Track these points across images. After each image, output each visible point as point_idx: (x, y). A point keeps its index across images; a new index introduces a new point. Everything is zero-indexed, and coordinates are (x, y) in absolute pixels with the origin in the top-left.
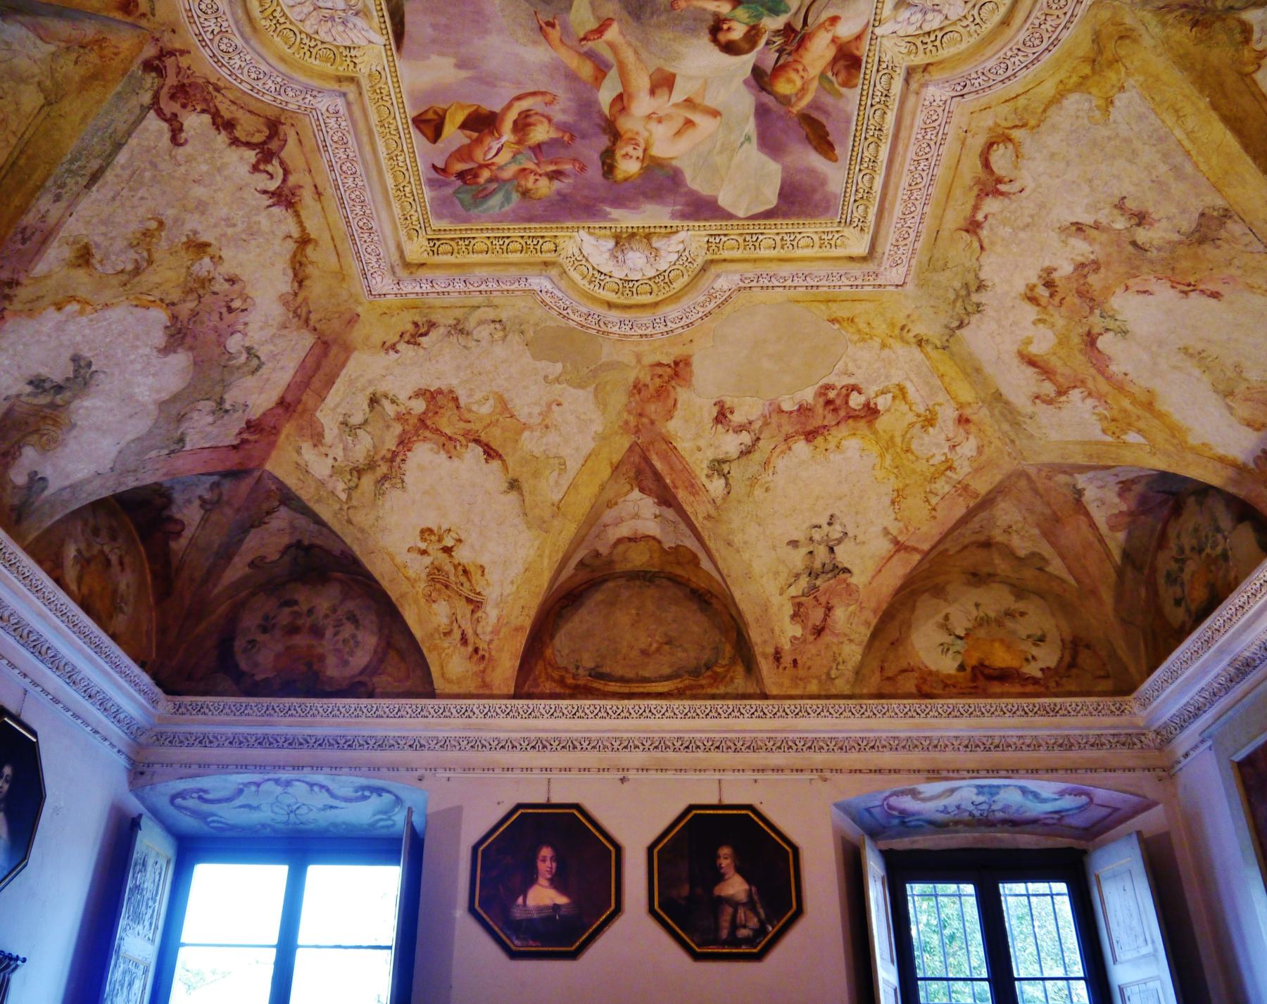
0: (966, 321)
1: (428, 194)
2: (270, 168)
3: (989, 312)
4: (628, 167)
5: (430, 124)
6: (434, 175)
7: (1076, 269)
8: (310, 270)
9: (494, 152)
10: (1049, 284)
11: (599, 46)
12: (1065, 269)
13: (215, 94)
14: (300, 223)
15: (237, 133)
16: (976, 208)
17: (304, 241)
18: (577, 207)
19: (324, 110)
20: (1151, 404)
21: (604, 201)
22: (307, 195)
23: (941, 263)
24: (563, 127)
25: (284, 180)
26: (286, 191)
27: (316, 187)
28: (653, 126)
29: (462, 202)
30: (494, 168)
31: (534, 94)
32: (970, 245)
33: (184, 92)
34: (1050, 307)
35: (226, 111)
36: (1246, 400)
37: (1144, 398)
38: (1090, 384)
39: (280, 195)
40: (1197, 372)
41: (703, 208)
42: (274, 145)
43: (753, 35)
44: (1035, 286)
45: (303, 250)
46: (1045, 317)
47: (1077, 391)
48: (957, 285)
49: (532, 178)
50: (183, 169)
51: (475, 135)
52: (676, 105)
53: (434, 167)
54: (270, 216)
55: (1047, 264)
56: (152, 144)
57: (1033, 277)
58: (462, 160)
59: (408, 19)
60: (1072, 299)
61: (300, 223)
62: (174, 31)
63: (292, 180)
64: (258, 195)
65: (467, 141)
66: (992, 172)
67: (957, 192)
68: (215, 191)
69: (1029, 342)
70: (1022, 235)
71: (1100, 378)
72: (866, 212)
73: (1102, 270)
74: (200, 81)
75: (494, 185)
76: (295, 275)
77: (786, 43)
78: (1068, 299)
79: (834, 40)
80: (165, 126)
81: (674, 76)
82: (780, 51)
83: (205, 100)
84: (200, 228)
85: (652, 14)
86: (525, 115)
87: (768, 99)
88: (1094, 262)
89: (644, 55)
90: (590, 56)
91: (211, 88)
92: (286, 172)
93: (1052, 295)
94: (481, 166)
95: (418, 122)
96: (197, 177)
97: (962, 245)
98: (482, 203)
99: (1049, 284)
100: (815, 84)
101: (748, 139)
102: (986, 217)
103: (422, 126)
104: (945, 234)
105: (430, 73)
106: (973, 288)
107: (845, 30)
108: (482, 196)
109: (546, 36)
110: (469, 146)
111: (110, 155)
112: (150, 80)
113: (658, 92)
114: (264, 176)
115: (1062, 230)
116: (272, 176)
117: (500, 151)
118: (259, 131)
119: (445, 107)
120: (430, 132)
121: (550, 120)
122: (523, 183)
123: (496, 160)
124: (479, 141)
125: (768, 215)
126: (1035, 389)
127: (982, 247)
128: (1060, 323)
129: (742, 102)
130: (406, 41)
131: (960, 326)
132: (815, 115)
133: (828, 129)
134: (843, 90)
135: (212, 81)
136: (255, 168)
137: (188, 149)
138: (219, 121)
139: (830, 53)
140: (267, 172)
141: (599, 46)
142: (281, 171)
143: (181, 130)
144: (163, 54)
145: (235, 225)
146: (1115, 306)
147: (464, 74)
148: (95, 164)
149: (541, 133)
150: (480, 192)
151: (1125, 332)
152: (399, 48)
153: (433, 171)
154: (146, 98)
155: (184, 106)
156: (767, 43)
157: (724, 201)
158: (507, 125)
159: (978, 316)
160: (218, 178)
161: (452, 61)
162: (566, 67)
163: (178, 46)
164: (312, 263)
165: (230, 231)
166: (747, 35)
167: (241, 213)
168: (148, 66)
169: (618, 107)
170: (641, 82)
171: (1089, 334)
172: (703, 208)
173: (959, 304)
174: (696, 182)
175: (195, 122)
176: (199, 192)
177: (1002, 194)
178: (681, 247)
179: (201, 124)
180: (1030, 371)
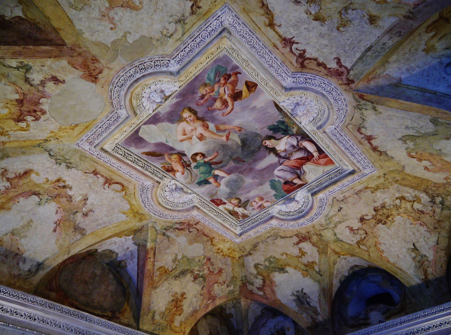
0: (52, 157)
1: (235, 62)
2: (299, 52)
3: (55, 166)
4: (186, 114)
5: (251, 86)
6: (238, 70)
7: (69, 195)
8: (262, 12)
9: (226, 90)
10: (64, 187)
11: (225, 134)
12: (70, 193)
13: (327, 74)
14: (277, 33)
15: (315, 62)
16: (102, 176)
17: (271, 25)
18: (187, 93)
19: (288, 78)
20: (3, 208)
21: (182, 101)
22: (280, 45)
23: (84, 160)
24: (214, 110)
25: (291, 48)
26: (289, 44)
27: (278, 49)
28: (192, 128)
29: (222, 67)
30: (222, 85)
31: (230, 113)
32: (88, 170)
33: (338, 74)
34: (54, 185)
35: (321, 69)
36: (12, 240)
37: (6, 206)
38: (12, 190)
39: (290, 42)
40: (21, 224)
41: (154, 120)
42: (300, 60)
43: (195, 160)
44: (65, 183)
45: (270, 21)
46: (49, 182)
47: (9, 185)
48: (72, 161)
49: (208, 91)
50: (333, 50)
51: (236, 91)
52: (193, 135)
53: (240, 73)
54: (291, 34)
55: (73, 188)
56: (347, 58)
57: (69, 182)
58: (233, 81)
59: (277, 110)
60: (56, 192)
61: (277, 33)
62: (346, 90)
63: (288, 49)
64: (299, 42)
65: (237, 88)
66: (113, 183)
67: (111, 173)
68: (318, 42)
69: (37, 174)
70: (87, 185)
71: (16, 194)
72: (120, 154)
73: (68, 202)
74: (333, 77)
75: (217, 80)
76: (267, 8)
77: (186, 164)
78: (57, 191)
79: (178, 171)
80: (343, 64)
81: (201, 141)
82: (185, 162)
83: (331, 72)
84: (320, 27)
85: (220, 148)
86: (227, 106)
87: (174, 152)
88: (71, 201)
89: (212, 140)
90: (224, 131)
91: (329, 75)
92: (291, 51)
93: (59, 187)
94: (226, 83)
95: (255, 85)
96: (327, 47)
97: (88, 167)
98: (215, 71)
99: (64, 187)
100: (169, 162)
101: (167, 142)
102: (98, 177)
103: (254, 84)
104: (96, 165)
105: (262, 100)
106: (68, 165)
107: (178, 175)
108: (217, 73)
109: (239, 127)
110: (235, 87)
111: (363, 56)
112: (351, 78)
113: (200, 135)
114: (300, 49)
115: (86, 195)
116: (296, 49)
117: (225, 91)
118: (308, 64)
119: (251, 94)
120: (250, 84)
121: (219, 110)
122: (209, 87)
123: (223, 88)
124: (233, 90)
125: (137, 132)
126: (10, 170)
127: (86, 173)
128: (46, 186)
129: (179, 147)
130: (274, 105)
131: (50, 154)
132: (161, 157)
133: (154, 158)
134: (163, 165)
135: (329, 77)
136: (304, 51)
137: (333, 57)
138: (323, 66)
139: (175, 169)
140: (299, 50)
141: (225, 134)
142: (294, 51)
143: (337, 63)
144: (348, 84)
145: (305, 29)
146: (51, 203)
147: (252, 105)
148: (369, 53)
149: (218, 104)
150: (219, 74)
151: (39, 204)
152: (274, 102)
153: (239, 71)
154: (351, 72)
155: (338, 70)
156: (190, 161)
157: (152, 126)
158: (229, 100)
159: (54, 162)
160: (318, 47)
161: (257, 107)
162: (227, 124)
163: (344, 86)
164: (263, 15)
165: (306, 26)
166: (196, 159)
167: (304, 34)
168: (353, 82)
169: (205, 125)
170: (206, 134)
171: (39, 194)
172: (154, 120)
173: (62, 158)
174: (166, 124)
175: (333, 65)
176: (325, 42)
177: (105, 184)
178: (147, 108)
179: (330, 65)
180: (22, 172)
